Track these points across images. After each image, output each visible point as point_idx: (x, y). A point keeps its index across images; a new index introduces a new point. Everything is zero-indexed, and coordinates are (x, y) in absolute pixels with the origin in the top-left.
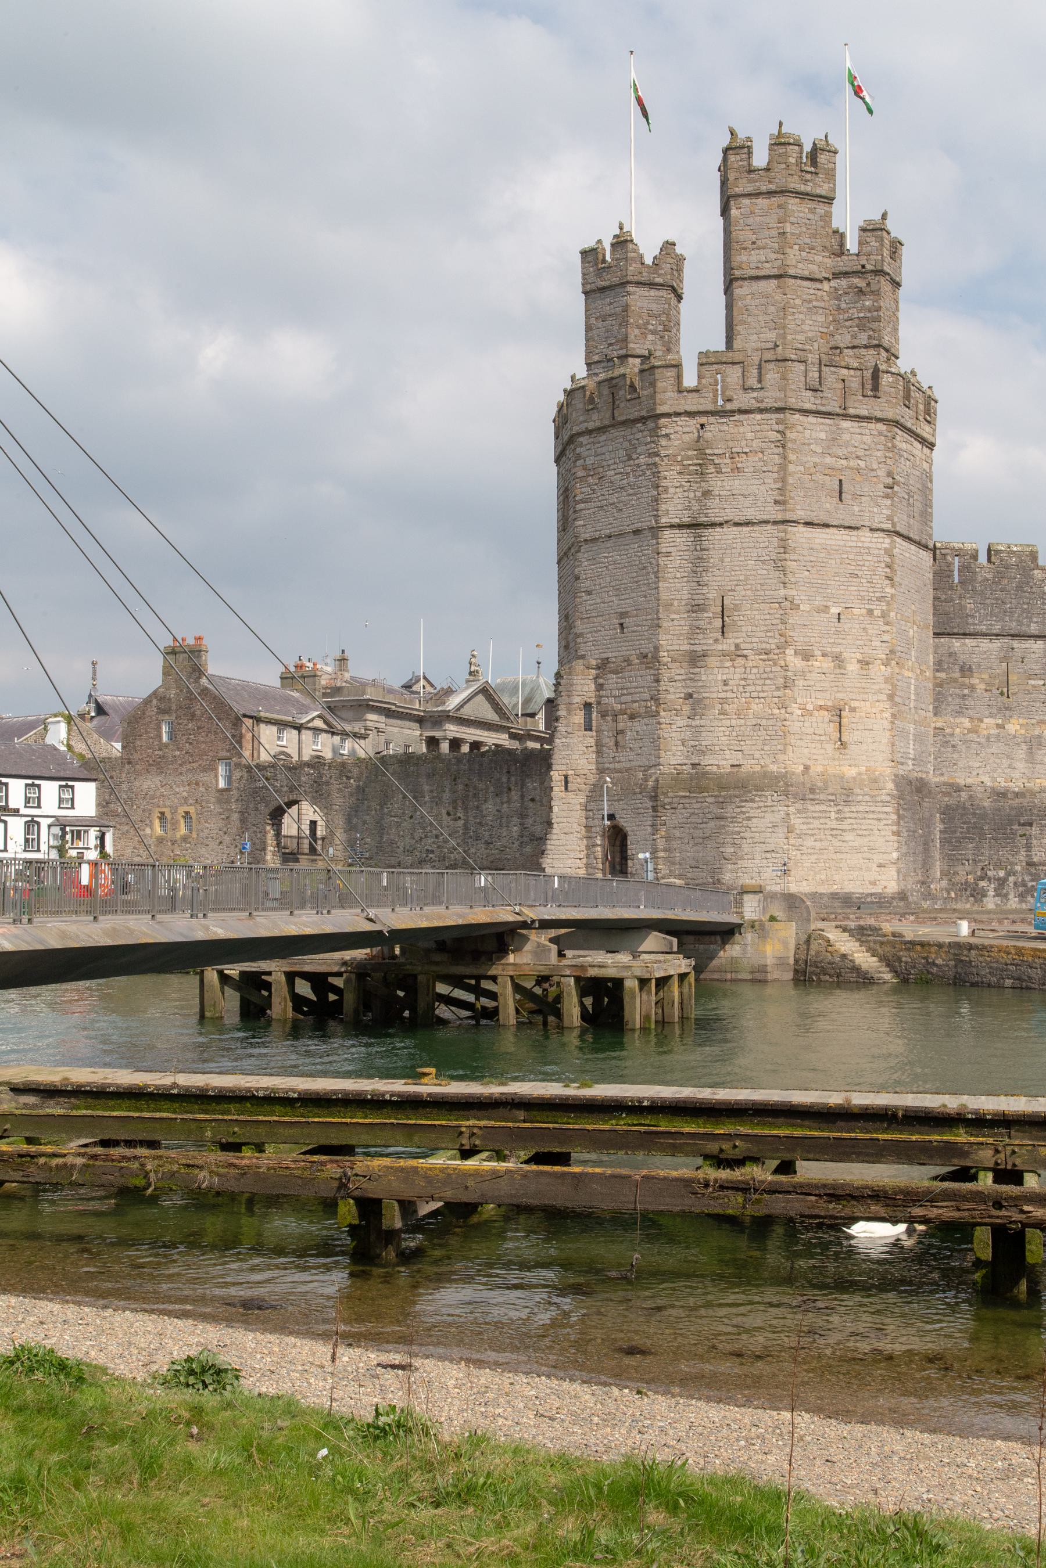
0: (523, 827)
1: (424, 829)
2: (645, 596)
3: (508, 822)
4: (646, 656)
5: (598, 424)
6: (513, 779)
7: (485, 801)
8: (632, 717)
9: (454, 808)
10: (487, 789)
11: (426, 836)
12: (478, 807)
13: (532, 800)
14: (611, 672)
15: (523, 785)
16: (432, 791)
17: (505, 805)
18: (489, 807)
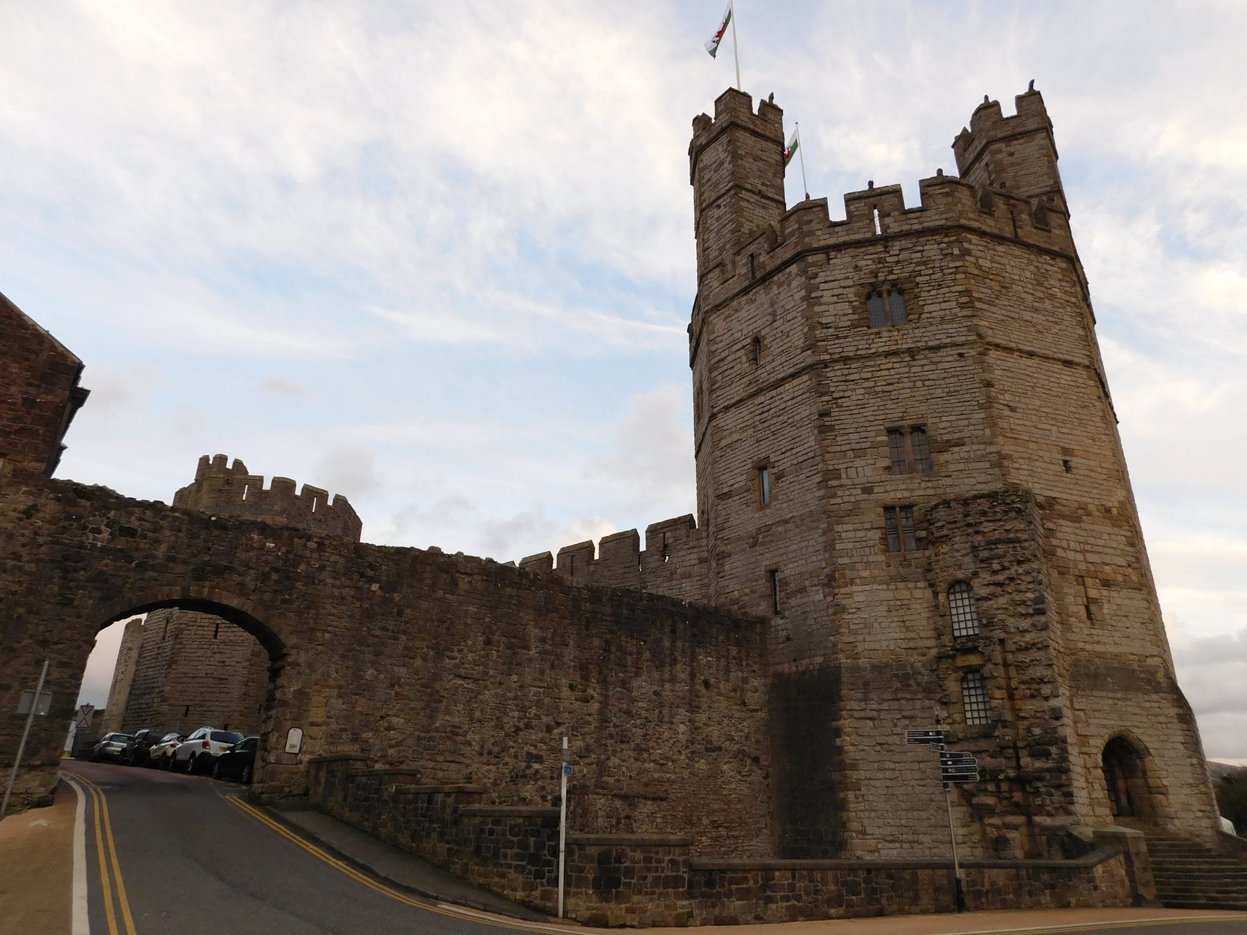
0: (694, 728)
1: (523, 709)
2: (1093, 439)
3: (672, 716)
4: (1108, 510)
5: (995, 231)
6: (679, 644)
7: (637, 675)
8: (1106, 584)
9: (586, 678)
10: (639, 653)
11: (528, 726)
12: (624, 683)
13: (707, 684)
14: (1064, 517)
15: (694, 657)
16: (543, 640)
17: (667, 686)
18: (643, 686)
